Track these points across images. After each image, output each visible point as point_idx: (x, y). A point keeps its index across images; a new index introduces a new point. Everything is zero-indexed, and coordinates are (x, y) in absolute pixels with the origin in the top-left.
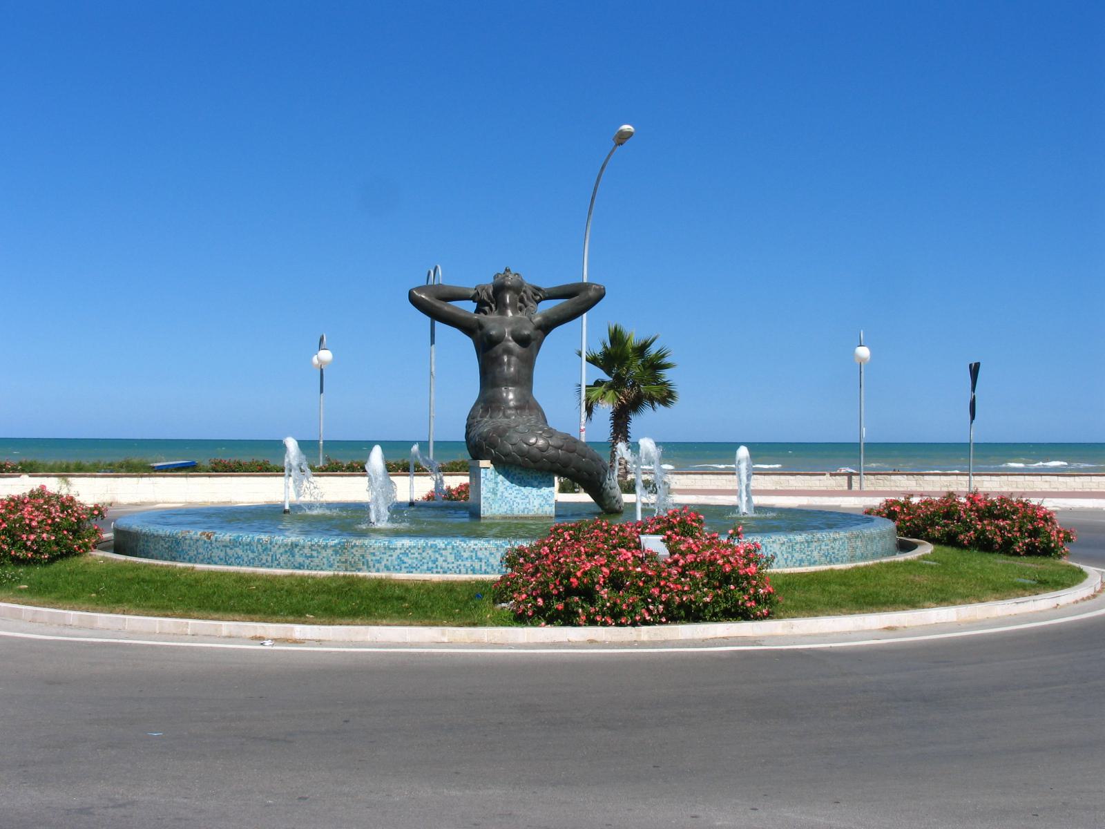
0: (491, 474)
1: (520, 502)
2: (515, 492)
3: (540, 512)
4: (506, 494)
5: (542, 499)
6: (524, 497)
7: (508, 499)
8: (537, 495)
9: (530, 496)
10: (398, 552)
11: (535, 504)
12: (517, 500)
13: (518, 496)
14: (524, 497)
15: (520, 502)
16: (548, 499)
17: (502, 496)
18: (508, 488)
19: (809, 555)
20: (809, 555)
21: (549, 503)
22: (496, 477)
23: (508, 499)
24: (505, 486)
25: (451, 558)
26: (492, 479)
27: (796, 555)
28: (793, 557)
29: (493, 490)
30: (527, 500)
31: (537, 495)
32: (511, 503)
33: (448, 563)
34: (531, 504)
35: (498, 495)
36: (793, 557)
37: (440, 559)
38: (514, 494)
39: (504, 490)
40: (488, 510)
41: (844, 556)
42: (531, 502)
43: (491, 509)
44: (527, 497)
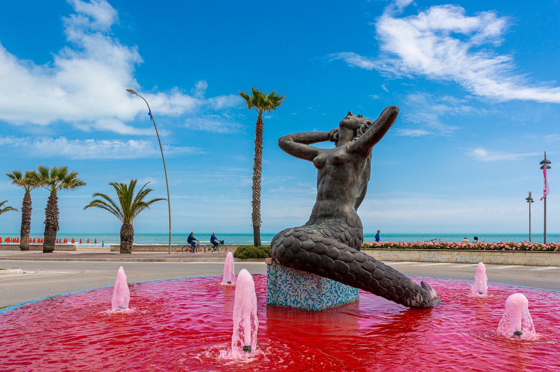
0: (273, 269)
1: (292, 294)
2: (289, 285)
3: (305, 306)
4: (282, 287)
5: (307, 293)
6: (293, 291)
7: (284, 291)
8: (303, 290)
9: (298, 290)
11: (302, 297)
12: (290, 292)
13: (290, 289)
14: (293, 291)
15: (292, 294)
16: (311, 294)
18: (284, 282)
21: (312, 297)
22: (277, 271)
23: (284, 291)
24: (281, 280)
26: (273, 274)
29: (274, 283)
30: (296, 294)
31: (303, 290)
32: (286, 295)
34: (299, 297)
35: (277, 288)
38: (288, 287)
39: (281, 283)
40: (271, 299)
42: (299, 295)
43: (273, 298)
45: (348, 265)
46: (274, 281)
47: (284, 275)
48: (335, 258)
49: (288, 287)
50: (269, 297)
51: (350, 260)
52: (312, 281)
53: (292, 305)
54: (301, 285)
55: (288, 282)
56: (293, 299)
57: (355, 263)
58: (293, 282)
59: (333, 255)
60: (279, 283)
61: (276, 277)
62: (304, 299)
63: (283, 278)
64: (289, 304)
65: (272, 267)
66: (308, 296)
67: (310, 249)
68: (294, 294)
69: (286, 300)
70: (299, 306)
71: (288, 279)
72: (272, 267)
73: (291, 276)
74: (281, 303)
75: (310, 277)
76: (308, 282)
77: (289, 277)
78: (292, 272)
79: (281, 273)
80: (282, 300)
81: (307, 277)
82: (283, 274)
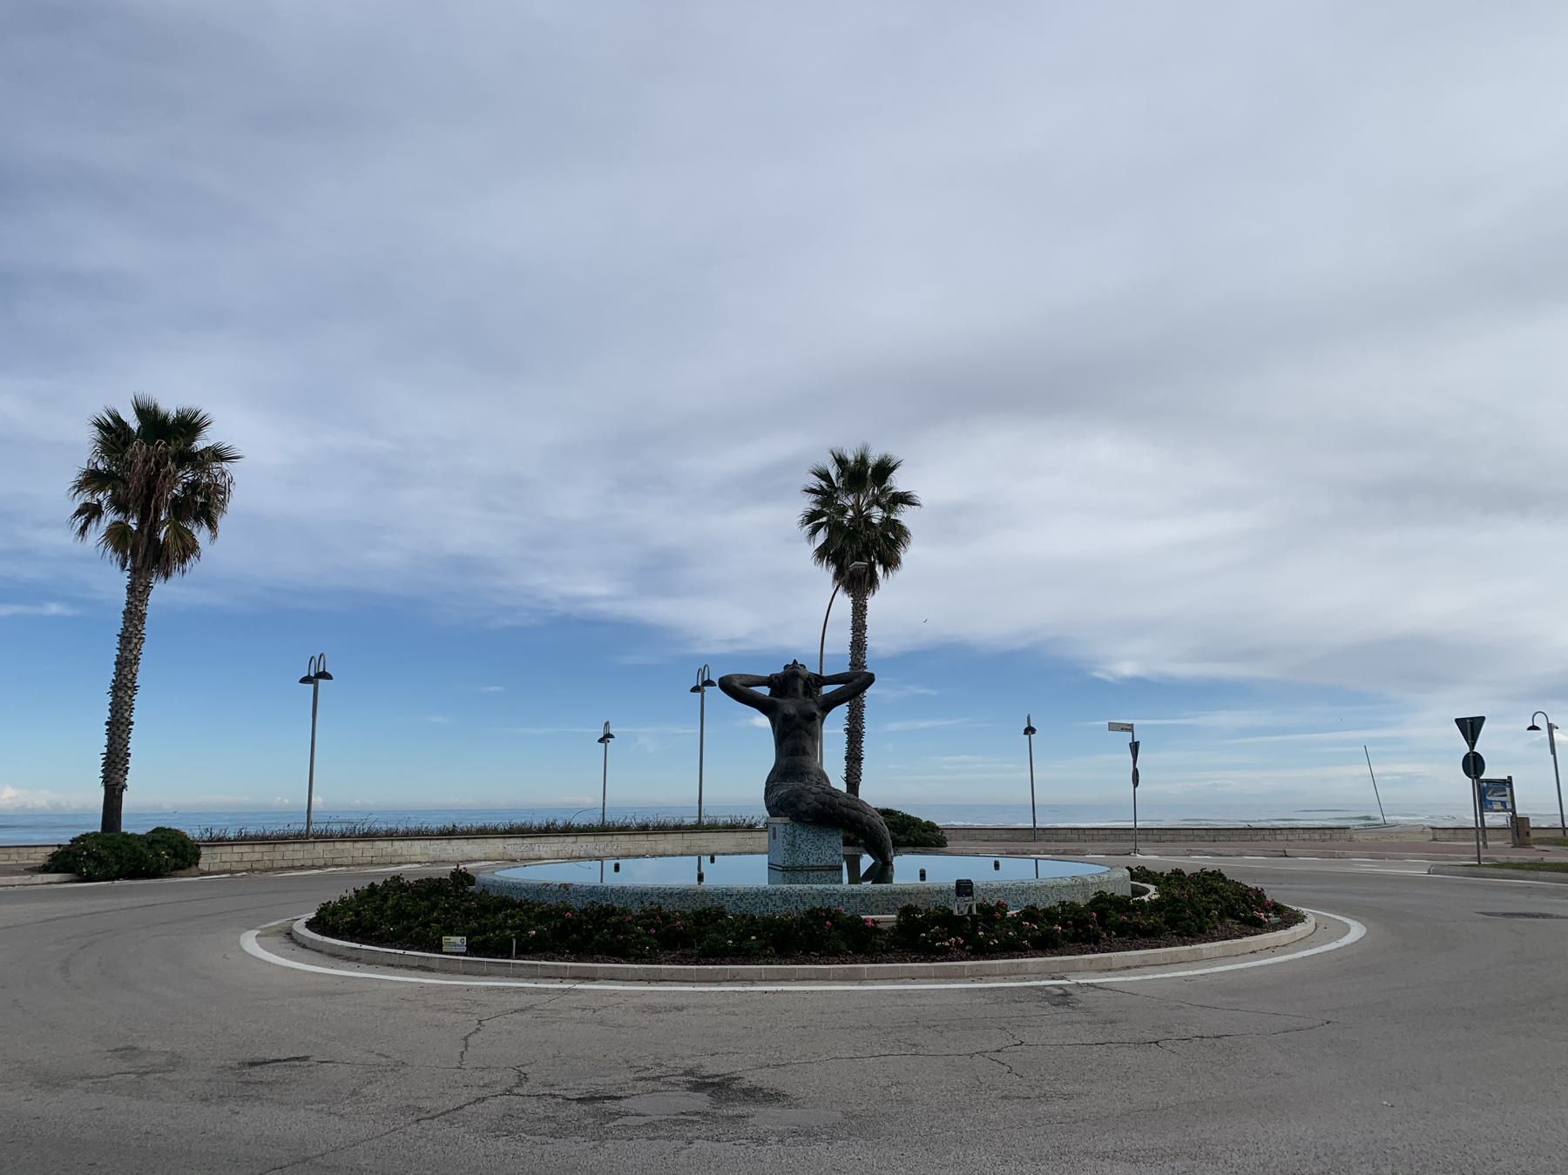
10: (734, 898)
12: (812, 851)
17: (799, 848)
22: (794, 831)
25: (779, 903)
33: (778, 907)
37: (771, 904)
44: (820, 848)
49: (809, 846)
53: (815, 864)
54: (826, 843)
56: (815, 857)
60: (798, 841)
61: (795, 837)
63: (803, 837)
64: (811, 863)
65: (788, 827)
70: (823, 864)
72: (788, 827)
76: (833, 839)
77: (811, 836)
78: (814, 831)
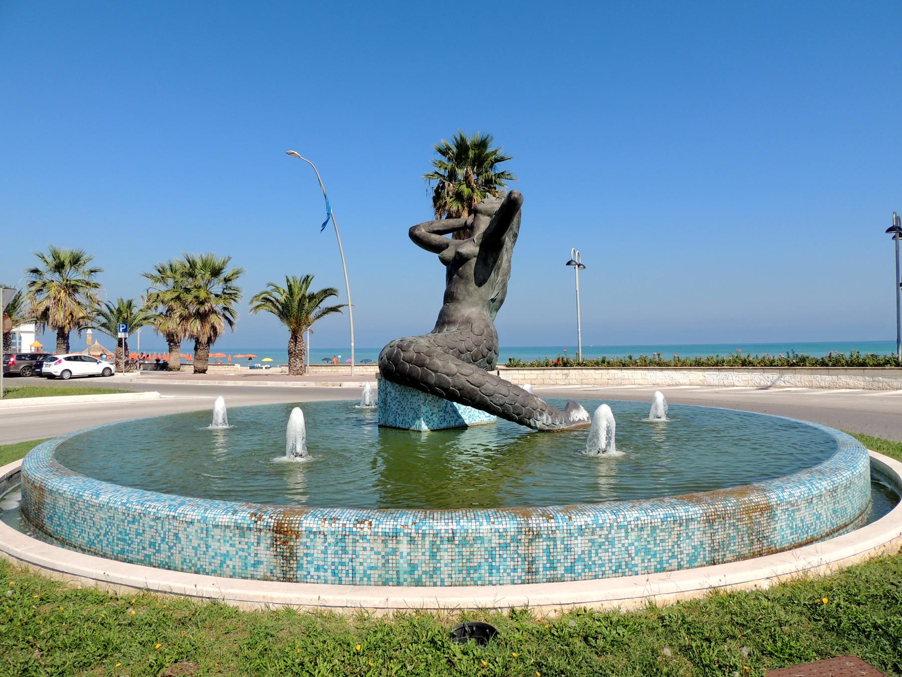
2: (398, 403)
4: (392, 405)
5: (414, 412)
6: (402, 409)
9: (406, 408)
12: (399, 411)
13: (399, 407)
15: (401, 413)
17: (389, 406)
19: (243, 550)
20: (243, 550)
27: (214, 545)
28: (207, 547)
30: (404, 412)
36: (207, 547)
38: (396, 405)
41: (343, 564)
45: (450, 380)
46: (385, 399)
47: (393, 391)
48: (436, 372)
49: (396, 405)
50: (380, 417)
51: (453, 373)
52: (418, 398)
55: (397, 400)
56: (401, 418)
57: (458, 376)
58: (401, 400)
59: (434, 368)
60: (389, 400)
61: (386, 394)
62: (411, 419)
66: (415, 416)
67: (410, 361)
68: (402, 413)
69: (396, 421)
71: (396, 396)
73: (399, 393)
74: (391, 424)
75: (417, 394)
76: (414, 399)
79: (390, 389)
80: (391, 420)
81: (413, 394)
82: (392, 391)
